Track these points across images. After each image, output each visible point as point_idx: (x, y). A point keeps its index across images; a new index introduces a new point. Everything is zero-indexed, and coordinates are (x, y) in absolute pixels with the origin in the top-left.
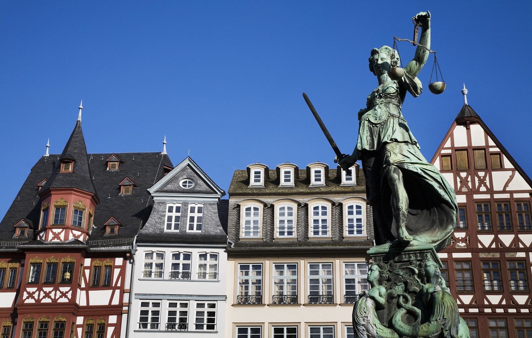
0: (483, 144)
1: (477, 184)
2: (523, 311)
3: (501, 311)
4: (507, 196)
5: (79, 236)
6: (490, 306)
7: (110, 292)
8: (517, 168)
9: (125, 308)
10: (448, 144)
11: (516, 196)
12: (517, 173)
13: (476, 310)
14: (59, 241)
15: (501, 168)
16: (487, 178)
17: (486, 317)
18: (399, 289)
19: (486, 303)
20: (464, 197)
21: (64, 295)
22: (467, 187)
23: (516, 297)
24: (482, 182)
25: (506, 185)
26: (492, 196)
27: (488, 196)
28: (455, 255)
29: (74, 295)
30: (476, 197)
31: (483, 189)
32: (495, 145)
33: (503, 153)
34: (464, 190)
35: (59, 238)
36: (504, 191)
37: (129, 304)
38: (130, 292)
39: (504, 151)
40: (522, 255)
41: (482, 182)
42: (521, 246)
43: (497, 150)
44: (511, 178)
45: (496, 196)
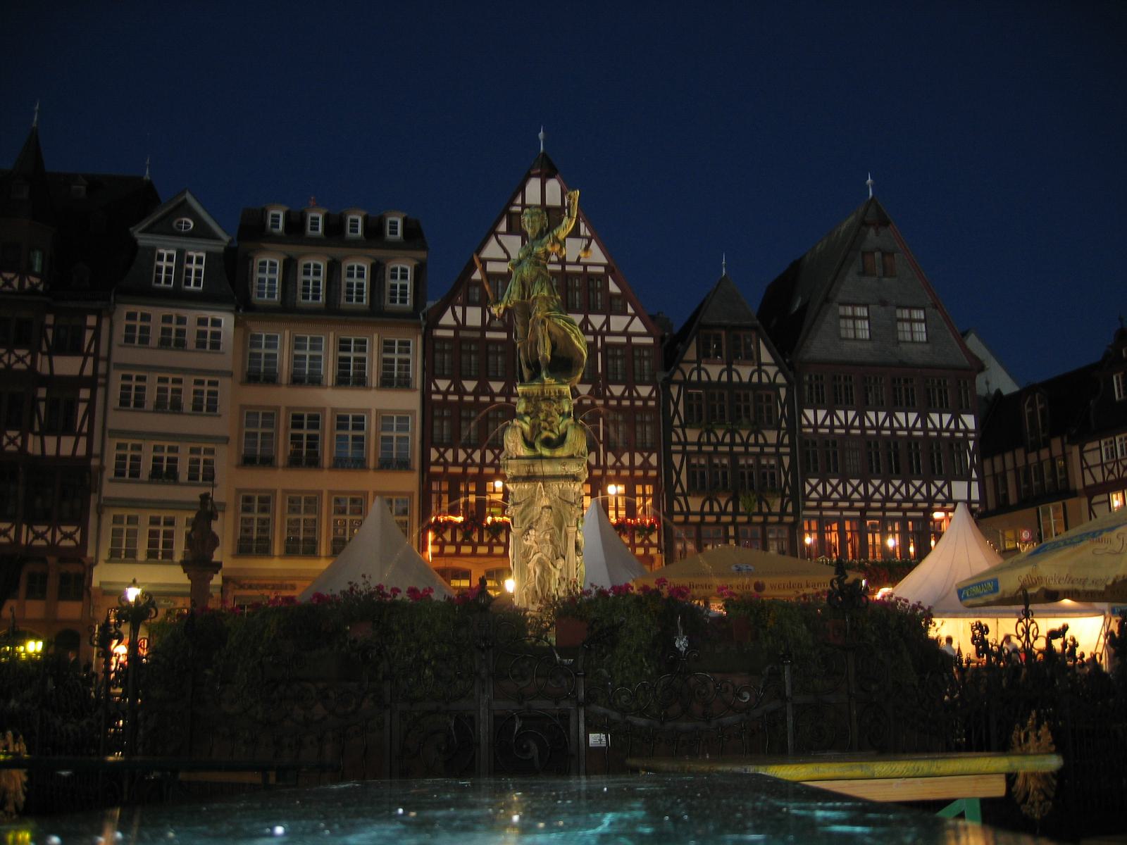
4: (580, 269)
5: (37, 285)
7: (79, 360)
9: (101, 380)
10: (519, 201)
11: (590, 269)
14: (11, 289)
21: (20, 359)
26: (563, 268)
27: (559, 268)
29: (34, 360)
35: (11, 285)
36: (578, 263)
37: (107, 376)
38: (108, 359)
42: (590, 328)
45: (568, 268)
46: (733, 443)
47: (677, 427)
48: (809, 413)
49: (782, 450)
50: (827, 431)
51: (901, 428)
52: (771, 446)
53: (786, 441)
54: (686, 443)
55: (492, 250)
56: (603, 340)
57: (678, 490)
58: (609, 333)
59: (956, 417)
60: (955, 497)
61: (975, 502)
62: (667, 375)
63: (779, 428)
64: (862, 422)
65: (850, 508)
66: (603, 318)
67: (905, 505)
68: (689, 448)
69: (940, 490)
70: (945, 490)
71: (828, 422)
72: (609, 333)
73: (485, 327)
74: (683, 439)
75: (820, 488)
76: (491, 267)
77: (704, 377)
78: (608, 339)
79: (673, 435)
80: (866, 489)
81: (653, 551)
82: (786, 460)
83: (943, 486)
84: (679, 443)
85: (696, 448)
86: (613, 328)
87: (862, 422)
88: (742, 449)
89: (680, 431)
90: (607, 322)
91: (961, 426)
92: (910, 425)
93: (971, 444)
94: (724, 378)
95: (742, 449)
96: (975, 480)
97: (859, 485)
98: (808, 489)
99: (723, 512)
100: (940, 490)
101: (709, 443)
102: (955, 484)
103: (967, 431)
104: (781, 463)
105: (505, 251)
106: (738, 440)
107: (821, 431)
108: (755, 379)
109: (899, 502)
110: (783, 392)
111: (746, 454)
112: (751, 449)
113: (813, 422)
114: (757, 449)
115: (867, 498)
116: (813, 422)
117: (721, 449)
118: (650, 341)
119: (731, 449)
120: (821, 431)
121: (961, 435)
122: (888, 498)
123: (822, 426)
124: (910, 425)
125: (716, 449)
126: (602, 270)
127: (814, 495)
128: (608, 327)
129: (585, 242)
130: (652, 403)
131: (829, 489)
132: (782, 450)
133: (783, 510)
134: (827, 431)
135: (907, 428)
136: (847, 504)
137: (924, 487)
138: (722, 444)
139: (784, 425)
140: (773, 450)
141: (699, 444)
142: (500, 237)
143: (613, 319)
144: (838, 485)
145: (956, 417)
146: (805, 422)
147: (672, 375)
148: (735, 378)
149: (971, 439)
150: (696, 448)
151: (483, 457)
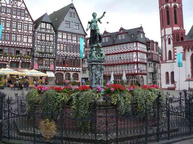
3: (15, 33)
4: (20, 8)
6: (13, 31)
11: (22, 8)
13: (10, 32)
15: (20, 1)
18: (97, 52)
20: (11, 6)
23: (19, 30)
24: (15, 3)
25: (20, 5)
27: (16, 7)
28: (7, 19)
30: (14, 6)
31: (15, 5)
36: (20, 7)
40: (21, 21)
41: (15, 3)
44: (22, 4)
45: (18, 7)
46: (45, 44)
48: (59, 39)
51: (73, 43)
53: (55, 44)
54: (37, 43)
57: (36, 51)
58: (25, 21)
65: (64, 56)
66: (24, 18)
67: (73, 56)
71: (62, 41)
72: (25, 21)
75: (60, 53)
78: (25, 22)
81: (30, 62)
82: (54, 47)
84: (36, 42)
85: (39, 44)
86: (26, 20)
88: (47, 45)
90: (25, 19)
94: (45, 32)
95: (47, 45)
98: (58, 52)
101: (41, 43)
104: (53, 48)
105: (6, 2)
110: (55, 35)
111: (48, 46)
114: (50, 45)
115: (67, 55)
117: (43, 44)
118: (32, 23)
122: (70, 55)
123: (61, 42)
126: (24, 9)
127: (59, 54)
129: (22, 3)
130: (32, 35)
133: (53, 56)
135: (74, 44)
139: (54, 41)
140: (52, 45)
143: (26, 18)
148: (47, 32)
150: (39, 44)
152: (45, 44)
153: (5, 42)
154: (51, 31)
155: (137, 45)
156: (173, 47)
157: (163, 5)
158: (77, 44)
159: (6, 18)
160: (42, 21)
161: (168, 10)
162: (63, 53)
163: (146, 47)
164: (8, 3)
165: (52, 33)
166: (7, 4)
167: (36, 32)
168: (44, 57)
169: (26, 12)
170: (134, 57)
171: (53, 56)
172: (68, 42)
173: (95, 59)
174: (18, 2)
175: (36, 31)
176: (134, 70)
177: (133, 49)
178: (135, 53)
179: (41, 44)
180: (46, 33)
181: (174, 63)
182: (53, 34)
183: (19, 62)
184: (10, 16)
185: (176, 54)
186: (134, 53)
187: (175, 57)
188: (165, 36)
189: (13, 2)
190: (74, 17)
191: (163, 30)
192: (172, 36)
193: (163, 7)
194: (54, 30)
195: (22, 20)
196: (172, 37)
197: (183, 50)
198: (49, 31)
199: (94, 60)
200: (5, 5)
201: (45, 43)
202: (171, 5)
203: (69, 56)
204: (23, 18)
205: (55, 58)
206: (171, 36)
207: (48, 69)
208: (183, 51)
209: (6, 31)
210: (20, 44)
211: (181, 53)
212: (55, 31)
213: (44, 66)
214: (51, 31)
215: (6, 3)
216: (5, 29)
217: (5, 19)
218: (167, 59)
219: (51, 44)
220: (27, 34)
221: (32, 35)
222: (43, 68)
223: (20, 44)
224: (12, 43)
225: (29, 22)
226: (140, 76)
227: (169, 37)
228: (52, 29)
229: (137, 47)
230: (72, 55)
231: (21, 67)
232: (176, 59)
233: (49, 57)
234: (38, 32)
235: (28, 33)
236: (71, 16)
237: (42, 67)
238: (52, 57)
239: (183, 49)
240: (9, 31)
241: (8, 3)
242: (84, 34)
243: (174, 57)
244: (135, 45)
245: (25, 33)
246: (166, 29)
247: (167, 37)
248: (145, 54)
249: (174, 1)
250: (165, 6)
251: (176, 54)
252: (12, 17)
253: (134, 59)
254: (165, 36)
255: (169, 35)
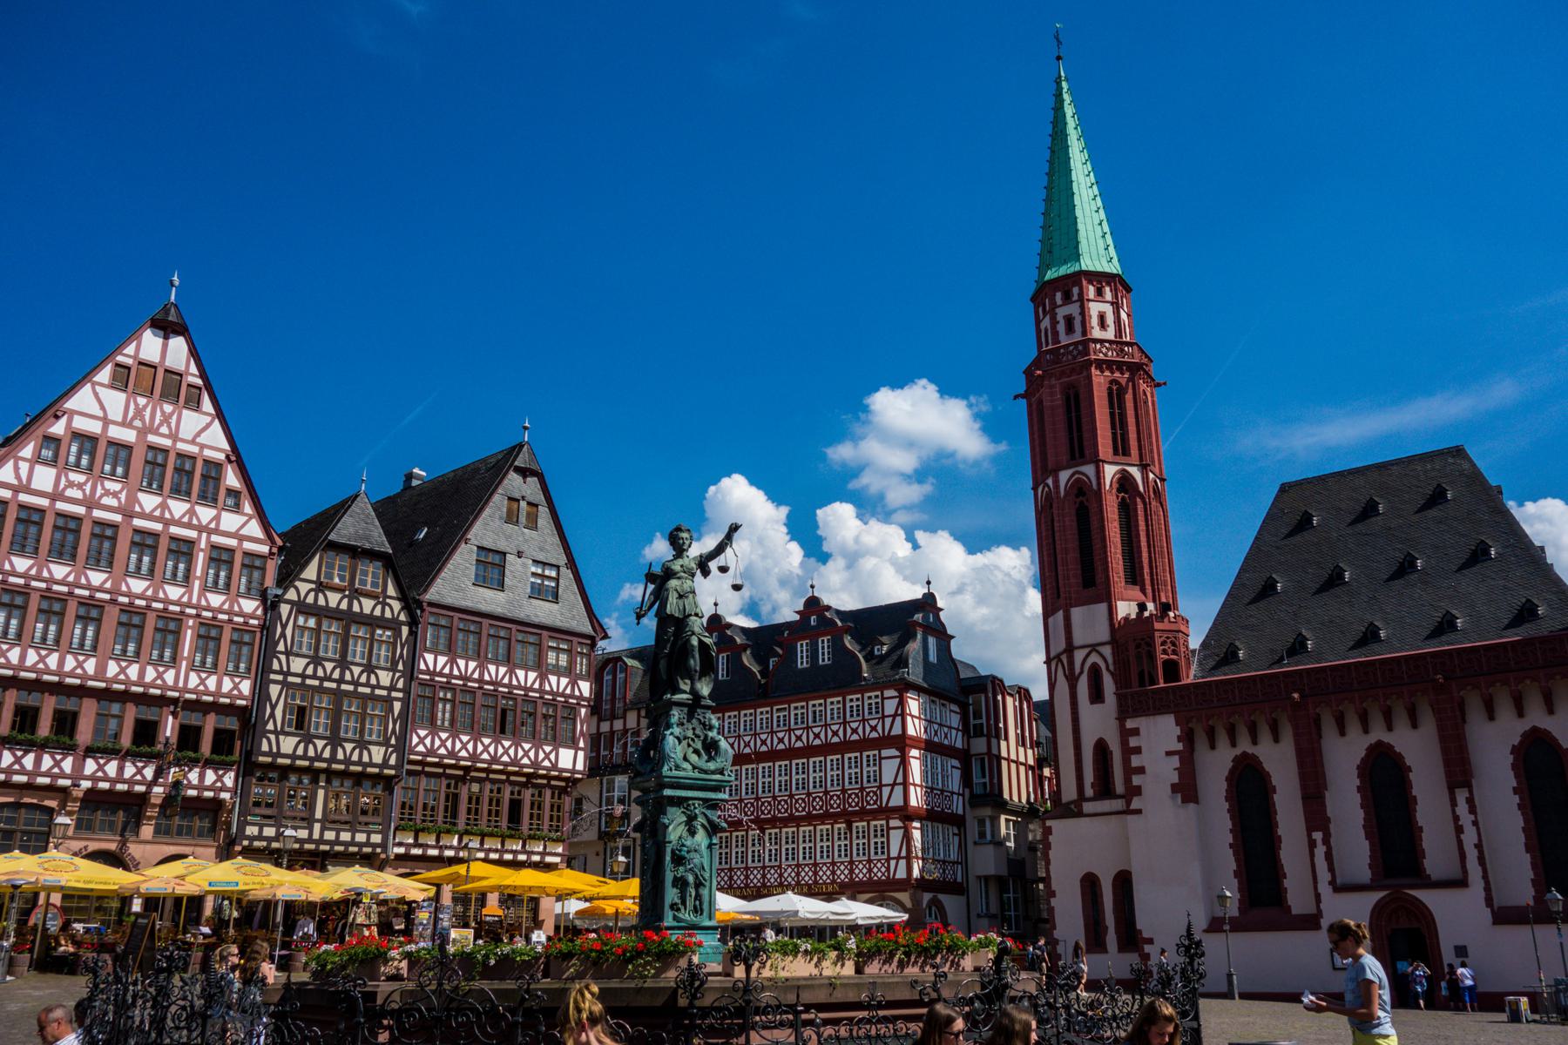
0: (181, 368)
1: (157, 422)
2: (172, 608)
4: (194, 449)
6: (129, 594)
8: (220, 414)
10: (130, 350)
11: (208, 453)
12: (217, 422)
16: (175, 417)
17: (118, 607)
19: (124, 588)
22: (143, 420)
24: (166, 419)
25: (198, 434)
27: (167, 442)
28: (97, 513)
31: (164, 430)
32: (197, 373)
33: (207, 389)
34: (138, 423)
36: (193, 442)
39: (208, 386)
41: (166, 419)
42: (195, 522)
43: (199, 382)
45: (180, 446)
46: (341, 681)
47: (281, 653)
48: (429, 657)
49: (394, 694)
50: (445, 680)
52: (383, 688)
53: (400, 685)
54: (288, 673)
55: (82, 400)
56: (208, 538)
57: (270, 726)
58: (217, 531)
59: (573, 683)
60: (561, 765)
61: (579, 772)
62: (279, 592)
63: (393, 669)
64: (482, 674)
68: (290, 679)
69: (547, 756)
70: (552, 757)
71: (447, 671)
72: (217, 531)
73: (55, 496)
74: (285, 669)
75: (428, 741)
76: (80, 424)
77: (321, 602)
78: (215, 539)
79: (275, 661)
80: (475, 748)
81: (225, 796)
82: (397, 706)
83: (551, 752)
84: (280, 672)
85: (298, 680)
86: (223, 527)
87: (482, 674)
88: (351, 688)
89: (283, 658)
90: (217, 518)
91: (577, 693)
92: (528, 685)
93: (583, 711)
94: (344, 606)
95: (351, 688)
96: (581, 749)
97: (468, 742)
98: (415, 740)
99: (319, 758)
100: (547, 756)
101: (314, 677)
102: (562, 751)
103: (581, 697)
104: (391, 709)
105: (103, 408)
106: (348, 677)
107: (437, 679)
108: (377, 612)
109: (506, 764)
110: (405, 630)
112: (361, 689)
113: (432, 669)
114: (367, 690)
115: (474, 757)
116: (431, 668)
117: (326, 684)
118: (265, 549)
119: (339, 686)
120: (437, 679)
121: (575, 701)
124: (528, 685)
125: (321, 684)
126: (222, 456)
127: (421, 748)
128: (218, 524)
129: (208, 419)
130: (255, 622)
131: (437, 743)
132: (394, 694)
134: (445, 680)
135: (525, 689)
136: (453, 762)
137: (533, 751)
138: (330, 679)
139: (400, 667)
140: (384, 693)
141: (303, 676)
142: (98, 388)
143: (224, 514)
144: (447, 739)
145: (573, 683)
146: (422, 666)
147: (284, 594)
148: (356, 608)
149: (584, 706)
150: (298, 680)
151: (23, 657)
152: (341, 681)
153: (61, 662)
154: (384, 604)
155: (902, 703)
156: (1121, 719)
157: (1055, 473)
158: (541, 691)
159: (90, 508)
160: (333, 537)
161: (1082, 502)
162: (449, 744)
163: (955, 720)
164: (116, 413)
165: (388, 614)
166: (106, 422)
167: (285, 609)
168: (324, 765)
169: (232, 479)
170: (888, 778)
171: (385, 764)
172: (487, 677)
173: (677, 767)
174: (185, 412)
175: (288, 602)
176: (889, 859)
177: (879, 728)
178: (894, 752)
179: (308, 682)
180: (348, 619)
181: (1130, 817)
182: (393, 624)
183: (144, 798)
184: (123, 496)
185: (1135, 761)
186: (885, 753)
187: (1136, 780)
188: (1070, 649)
189: (149, 410)
190: (535, 528)
191: (1060, 614)
192: (1113, 654)
193: (1056, 482)
194: (403, 597)
195: (201, 529)
196: (1110, 660)
197: (1180, 739)
198: (368, 605)
199: (675, 773)
200: (94, 427)
201: (336, 675)
202: (1099, 474)
203: (489, 763)
204: (205, 514)
205: (391, 777)
206: (1107, 651)
207: (340, 848)
208: (1180, 747)
209: (78, 591)
210: (169, 677)
211: (1169, 754)
212: (407, 607)
213: (317, 826)
214: (384, 604)
215: (100, 414)
216: (77, 578)
217: (81, 510)
218: (1089, 792)
219: (379, 686)
220: (225, 617)
221: (255, 622)
222: (310, 840)
223: (170, 682)
224: (112, 669)
225: (242, 538)
226: (927, 897)
227: (1094, 658)
228: (391, 591)
229: (903, 716)
230: (505, 759)
231: (157, 831)
232: (1137, 791)
233: (359, 769)
234: (301, 608)
235: (229, 612)
236: (512, 518)
237: (303, 834)
238: (376, 770)
239: (1177, 731)
240: (100, 589)
241: (116, 413)
242: (587, 628)
243: (1128, 780)
244: (890, 707)
245: (208, 609)
246: (1077, 613)
247: (1079, 656)
248: (956, 763)
249: (1116, 452)
250: (1064, 476)
251: (1135, 761)
252: (132, 499)
253: (886, 791)
254: (1070, 649)
255: (1093, 648)
